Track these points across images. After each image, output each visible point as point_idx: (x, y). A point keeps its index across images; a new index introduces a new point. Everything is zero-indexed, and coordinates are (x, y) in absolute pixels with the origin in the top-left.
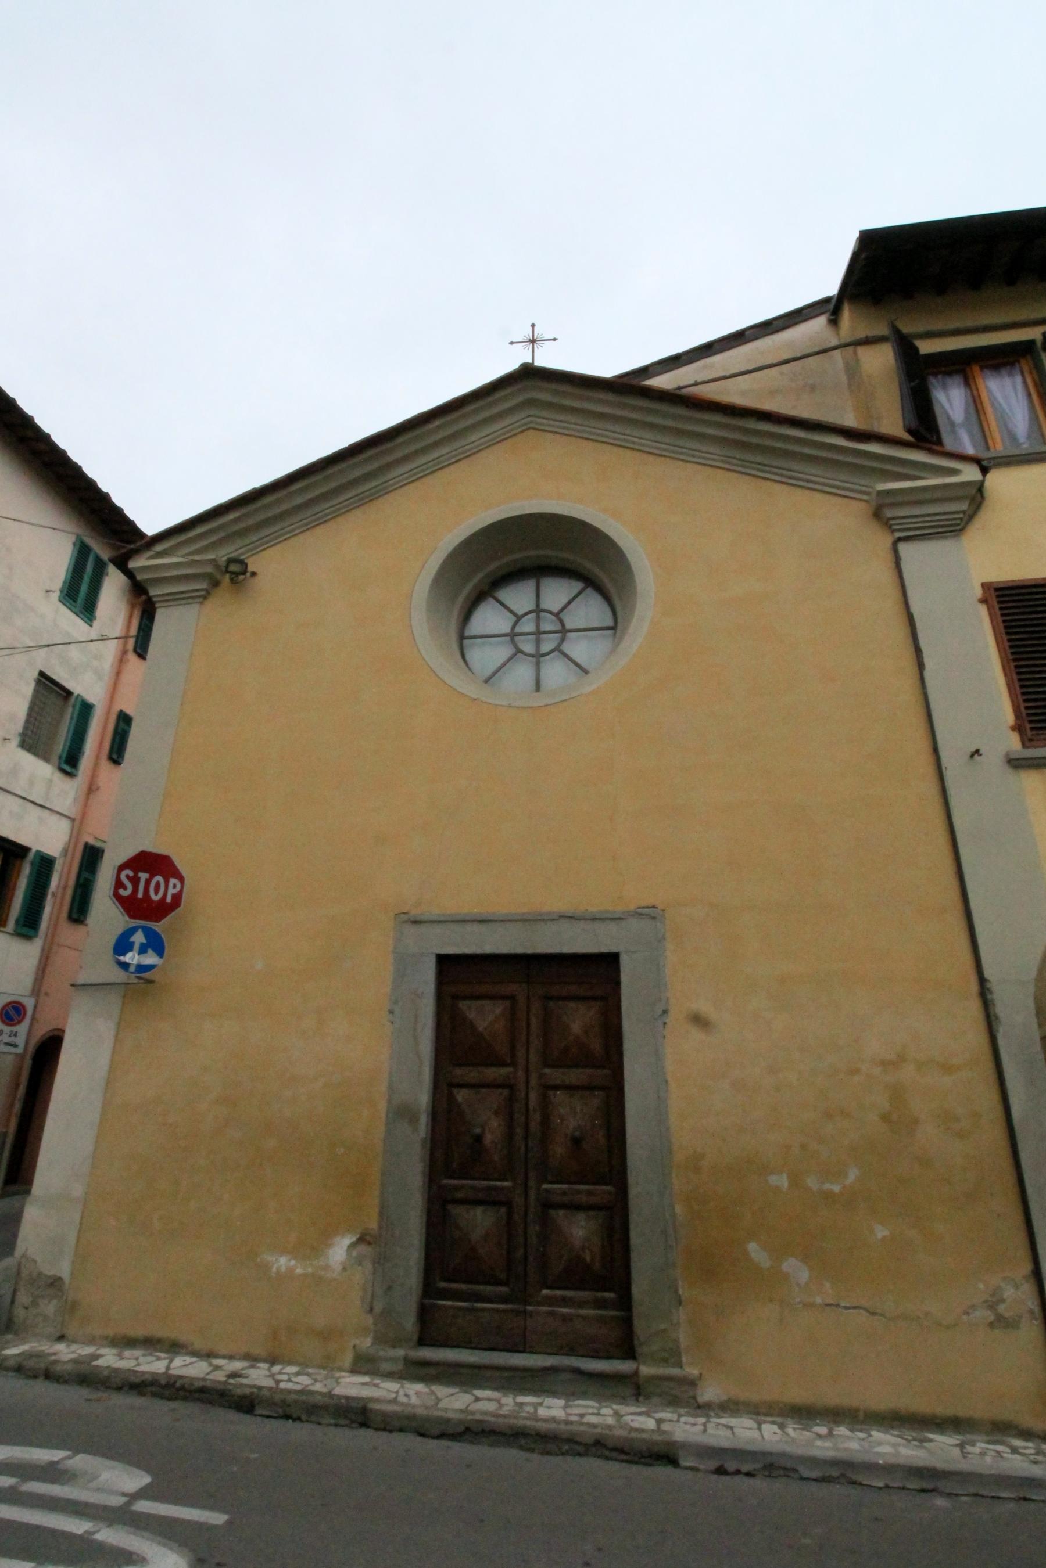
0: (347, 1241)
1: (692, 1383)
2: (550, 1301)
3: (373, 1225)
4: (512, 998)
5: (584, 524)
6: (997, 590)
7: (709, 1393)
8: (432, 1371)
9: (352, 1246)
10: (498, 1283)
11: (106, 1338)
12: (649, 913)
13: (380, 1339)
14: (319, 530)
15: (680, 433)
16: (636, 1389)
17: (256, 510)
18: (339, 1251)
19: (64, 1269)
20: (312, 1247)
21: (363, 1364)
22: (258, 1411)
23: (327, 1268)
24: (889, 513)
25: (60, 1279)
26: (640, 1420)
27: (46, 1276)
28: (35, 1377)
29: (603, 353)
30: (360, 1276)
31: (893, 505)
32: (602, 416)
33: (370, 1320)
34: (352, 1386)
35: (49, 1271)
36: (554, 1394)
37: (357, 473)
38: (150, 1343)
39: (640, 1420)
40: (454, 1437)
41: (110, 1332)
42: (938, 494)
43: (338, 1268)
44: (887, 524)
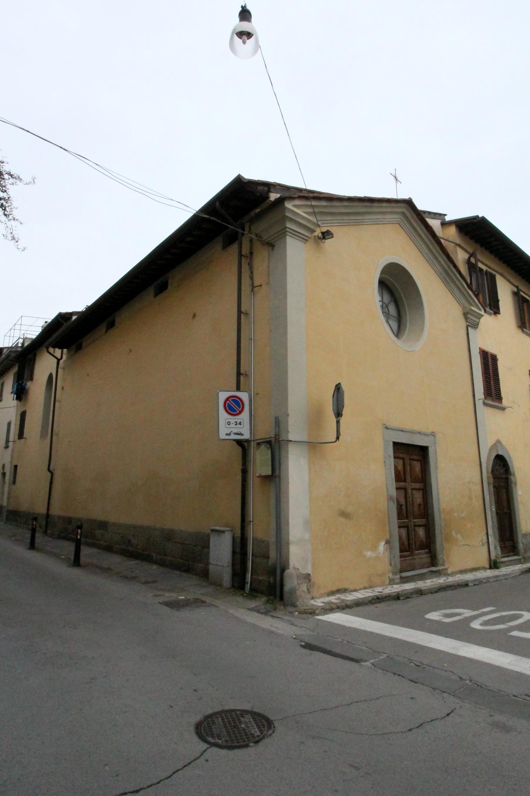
0: (383, 543)
1: (446, 569)
2: (419, 554)
3: (388, 537)
4: (403, 459)
5: (410, 277)
6: (483, 351)
7: (449, 571)
8: (405, 580)
9: (384, 545)
10: (407, 551)
11: (326, 593)
12: (433, 434)
13: (394, 573)
14: (345, 228)
15: (436, 258)
16: (438, 574)
17: (340, 206)
18: (382, 546)
19: (309, 570)
20: (374, 548)
21: (392, 582)
22: (401, 598)
23: (379, 553)
24: (469, 316)
25: (309, 574)
26: (441, 581)
27: (304, 574)
28: (352, 607)
29: (421, 206)
30: (387, 554)
31: (472, 315)
32: (420, 235)
33: (390, 568)
34: (397, 588)
35: (304, 572)
36: (427, 579)
37: (423, 235)
38: (338, 591)
39: (441, 581)
40: (436, 592)
41: (326, 591)
42: (476, 315)
43: (382, 553)
44: (466, 319)
